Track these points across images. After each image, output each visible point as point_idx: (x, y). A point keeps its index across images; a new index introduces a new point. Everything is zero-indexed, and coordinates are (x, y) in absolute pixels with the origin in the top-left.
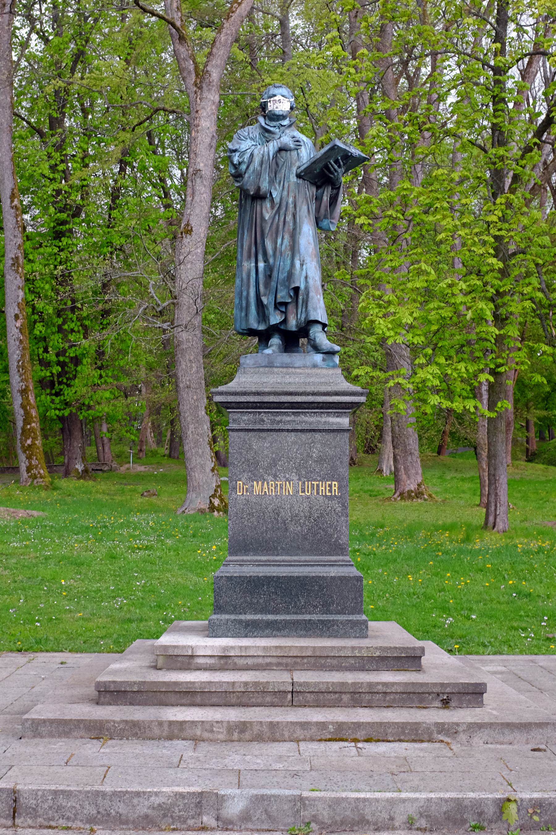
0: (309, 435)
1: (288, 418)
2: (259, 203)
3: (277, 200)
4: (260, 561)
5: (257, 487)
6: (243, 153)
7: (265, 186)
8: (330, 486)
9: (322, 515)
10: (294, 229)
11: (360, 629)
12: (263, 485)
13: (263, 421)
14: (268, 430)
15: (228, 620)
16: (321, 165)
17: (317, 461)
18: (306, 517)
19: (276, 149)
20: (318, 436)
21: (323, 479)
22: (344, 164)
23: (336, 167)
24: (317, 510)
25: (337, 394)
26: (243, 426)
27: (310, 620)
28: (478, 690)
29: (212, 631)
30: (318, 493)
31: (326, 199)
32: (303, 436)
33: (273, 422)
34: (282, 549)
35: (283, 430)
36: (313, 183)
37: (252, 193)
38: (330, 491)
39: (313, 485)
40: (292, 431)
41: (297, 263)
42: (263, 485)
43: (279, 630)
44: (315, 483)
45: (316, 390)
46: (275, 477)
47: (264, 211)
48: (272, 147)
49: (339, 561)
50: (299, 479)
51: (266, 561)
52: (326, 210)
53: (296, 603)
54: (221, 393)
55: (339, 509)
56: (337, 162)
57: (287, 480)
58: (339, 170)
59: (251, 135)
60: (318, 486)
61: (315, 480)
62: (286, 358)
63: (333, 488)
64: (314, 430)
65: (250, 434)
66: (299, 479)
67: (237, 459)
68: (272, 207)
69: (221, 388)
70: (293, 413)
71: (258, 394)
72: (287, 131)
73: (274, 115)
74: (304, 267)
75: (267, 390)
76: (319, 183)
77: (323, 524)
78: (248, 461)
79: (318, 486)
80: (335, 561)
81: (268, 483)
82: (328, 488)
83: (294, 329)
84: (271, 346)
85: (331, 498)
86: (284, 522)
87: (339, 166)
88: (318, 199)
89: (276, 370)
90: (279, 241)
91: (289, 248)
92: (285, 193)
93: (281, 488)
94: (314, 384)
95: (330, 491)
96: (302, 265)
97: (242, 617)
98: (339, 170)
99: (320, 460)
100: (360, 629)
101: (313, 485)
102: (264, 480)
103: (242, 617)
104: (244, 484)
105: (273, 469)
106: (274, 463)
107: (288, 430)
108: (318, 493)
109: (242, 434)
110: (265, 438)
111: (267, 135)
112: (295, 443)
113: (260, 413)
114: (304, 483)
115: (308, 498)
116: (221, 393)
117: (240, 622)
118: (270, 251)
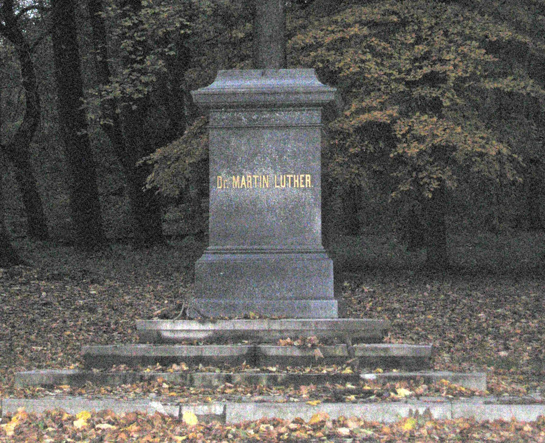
5: (235, 181)
8: (304, 179)
21: (296, 173)
30: (292, 185)
38: (304, 183)
39: (287, 179)
44: (290, 176)
50: (275, 173)
57: (264, 174)
60: (292, 179)
61: (290, 173)
63: (307, 180)
66: (275, 173)
78: (228, 156)
79: (292, 179)
82: (302, 181)
95: (304, 183)
99: (295, 155)
101: (287, 179)
102: (242, 174)
105: (249, 164)
108: (292, 185)
112: (270, 139)
114: (279, 176)
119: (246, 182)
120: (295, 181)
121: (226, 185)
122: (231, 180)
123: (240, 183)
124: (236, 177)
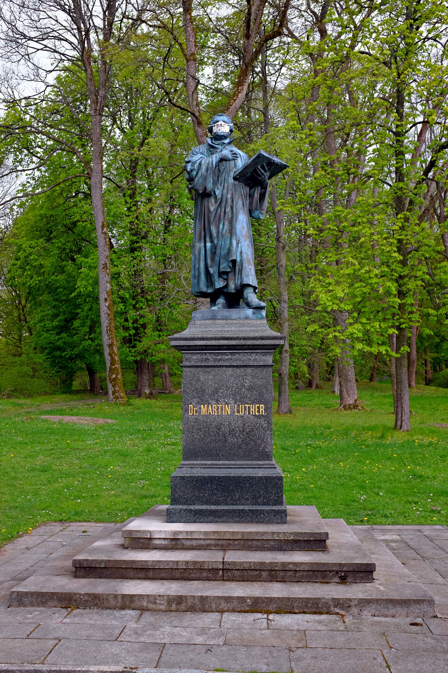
0: (242, 369)
1: (227, 357)
2: (206, 199)
3: (219, 197)
4: (206, 465)
5: (204, 409)
6: (194, 163)
7: (210, 186)
8: (259, 408)
9: (252, 430)
10: (232, 217)
11: (281, 517)
12: (208, 407)
13: (208, 359)
14: (212, 366)
15: (181, 509)
16: (251, 170)
17: (248, 389)
18: (240, 431)
19: (218, 159)
20: (249, 370)
21: (253, 403)
22: (269, 170)
23: (262, 171)
24: (249, 426)
25: (262, 338)
26: (193, 363)
27: (243, 510)
28: (368, 569)
29: (170, 517)
30: (249, 413)
31: (257, 195)
32: (238, 371)
33: (215, 360)
34: (223, 455)
35: (222, 366)
36: (247, 185)
37: (201, 192)
38: (259, 412)
39: (245, 407)
40: (230, 366)
41: (234, 242)
42: (208, 407)
43: (219, 517)
44: (247, 406)
45: (246, 336)
46: (217, 401)
47: (210, 205)
48: (215, 158)
49: (266, 464)
50: (235, 403)
51: (210, 465)
52: (257, 204)
53: (232, 496)
54: (176, 339)
55: (266, 425)
56: (263, 167)
58: (265, 174)
59: (201, 151)
60: (249, 408)
61: (247, 404)
62: (227, 312)
64: (246, 366)
65: (199, 369)
66: (235, 403)
67: (188, 388)
68: (216, 202)
69: (176, 336)
70: (230, 353)
71: (203, 339)
72: (228, 147)
73: (218, 135)
74: (240, 245)
75: (209, 336)
76: (251, 185)
77: (253, 437)
78: (197, 389)
79: (249, 408)
80: (263, 465)
81: (212, 406)
82: (257, 410)
83: (233, 291)
84: (218, 304)
85: (259, 417)
86: (224, 435)
87: (265, 171)
88: (251, 196)
89: (218, 321)
90: (221, 226)
91: (228, 231)
92: (225, 191)
93: (222, 409)
94: (246, 331)
95: (259, 412)
96: (238, 244)
97: (192, 507)
98: (265, 174)
99: (251, 389)
100: (281, 517)
101: (245, 407)
102: (209, 404)
103: (192, 507)
104: (194, 406)
105: (215, 396)
106: (216, 391)
107: (226, 366)
108: (249, 413)
109: (192, 369)
110: (209, 372)
111: (212, 150)
112: (231, 376)
113: (206, 353)
114: (239, 406)
115: (242, 417)
116: (176, 339)
117: (190, 511)
118: (215, 234)
119: (212, 410)
120: (251, 410)
121: (196, 412)
122: (200, 408)
123: (207, 411)
124: (204, 406)
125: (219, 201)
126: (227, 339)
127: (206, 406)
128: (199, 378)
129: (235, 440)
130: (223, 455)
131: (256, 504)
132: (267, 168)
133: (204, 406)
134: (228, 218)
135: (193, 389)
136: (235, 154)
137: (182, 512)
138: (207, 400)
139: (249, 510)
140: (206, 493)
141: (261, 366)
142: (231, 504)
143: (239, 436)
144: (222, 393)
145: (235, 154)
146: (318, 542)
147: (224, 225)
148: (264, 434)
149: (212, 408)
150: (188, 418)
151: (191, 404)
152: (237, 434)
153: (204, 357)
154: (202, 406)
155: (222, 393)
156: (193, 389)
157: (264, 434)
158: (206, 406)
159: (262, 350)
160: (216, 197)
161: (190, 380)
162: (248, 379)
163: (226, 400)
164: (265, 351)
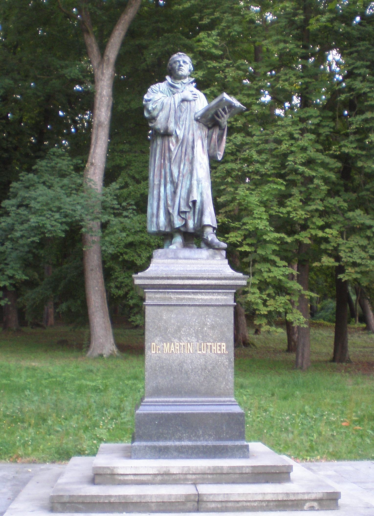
0: (205, 308)
1: (190, 297)
2: (166, 138)
3: (181, 137)
4: (169, 402)
5: (166, 347)
6: (156, 102)
7: (172, 126)
8: (220, 346)
9: (214, 367)
10: (193, 158)
11: (244, 452)
12: (170, 345)
13: (171, 298)
14: (174, 305)
15: (146, 446)
16: (213, 112)
17: (210, 328)
18: (202, 369)
19: (180, 100)
20: (211, 309)
22: (229, 112)
23: (223, 113)
24: (211, 364)
25: (225, 279)
26: (155, 302)
27: (207, 446)
28: (334, 497)
30: (211, 351)
31: (215, 137)
32: (200, 309)
33: (178, 299)
34: (185, 392)
35: (185, 305)
36: (207, 126)
37: (162, 131)
40: (192, 305)
41: (195, 182)
42: (170, 345)
43: (183, 453)
44: (209, 344)
45: (210, 276)
46: (180, 339)
47: (171, 145)
48: (178, 97)
49: (227, 401)
50: (197, 341)
51: (173, 402)
52: (215, 145)
53: (196, 433)
54: (140, 278)
55: (227, 363)
56: (224, 110)
57: (189, 341)
58: (225, 116)
59: (161, 90)
60: (211, 346)
61: (209, 342)
62: (187, 252)
63: (222, 348)
64: (208, 305)
65: (162, 308)
66: (197, 341)
67: (151, 326)
68: (177, 141)
69: (140, 274)
70: (193, 292)
71: (168, 278)
72: (187, 87)
74: (200, 185)
75: (174, 276)
76: (210, 126)
77: (215, 374)
78: (160, 327)
79: (211, 346)
80: (224, 402)
81: (174, 344)
82: (218, 348)
83: (192, 231)
84: (175, 243)
85: (221, 355)
86: (186, 373)
87: (226, 113)
88: (209, 137)
89: (180, 261)
90: (182, 166)
91: (189, 171)
92: (187, 133)
93: (184, 348)
94: (208, 271)
95: (220, 350)
96: (198, 184)
97: (156, 444)
98: (225, 116)
99: (213, 327)
100: (244, 452)
102: (172, 342)
103: (156, 444)
104: (156, 345)
106: (179, 329)
107: (189, 305)
108: (211, 351)
109: (155, 308)
110: (172, 311)
111: (172, 89)
112: (194, 315)
113: (168, 292)
114: (201, 344)
115: (204, 355)
116: (140, 278)
117: (155, 447)
118: (176, 174)
119: (175, 348)
120: (213, 348)
121: (159, 350)
122: (163, 346)
123: (170, 349)
124: (167, 344)
125: (180, 141)
126: (208, 279)
127: (168, 344)
128: (161, 316)
129: (197, 377)
130: (185, 392)
131: (220, 439)
132: (227, 111)
133: (167, 344)
134: (188, 159)
135: (156, 327)
136: (195, 94)
137: (147, 448)
138: (170, 339)
139: (213, 446)
140: (170, 430)
141: (223, 306)
142: (194, 440)
143: (201, 374)
144: (184, 331)
145: (195, 94)
146: (279, 475)
147: (184, 165)
148: (226, 372)
149: (174, 346)
150: (151, 356)
151: (154, 342)
152: (199, 372)
153: (167, 296)
154: (165, 344)
155: (184, 331)
156: (156, 327)
157: (226, 372)
158: (168, 344)
159: (224, 289)
160: (177, 137)
161: (153, 319)
162: (210, 319)
163: (189, 339)
164: (227, 291)
